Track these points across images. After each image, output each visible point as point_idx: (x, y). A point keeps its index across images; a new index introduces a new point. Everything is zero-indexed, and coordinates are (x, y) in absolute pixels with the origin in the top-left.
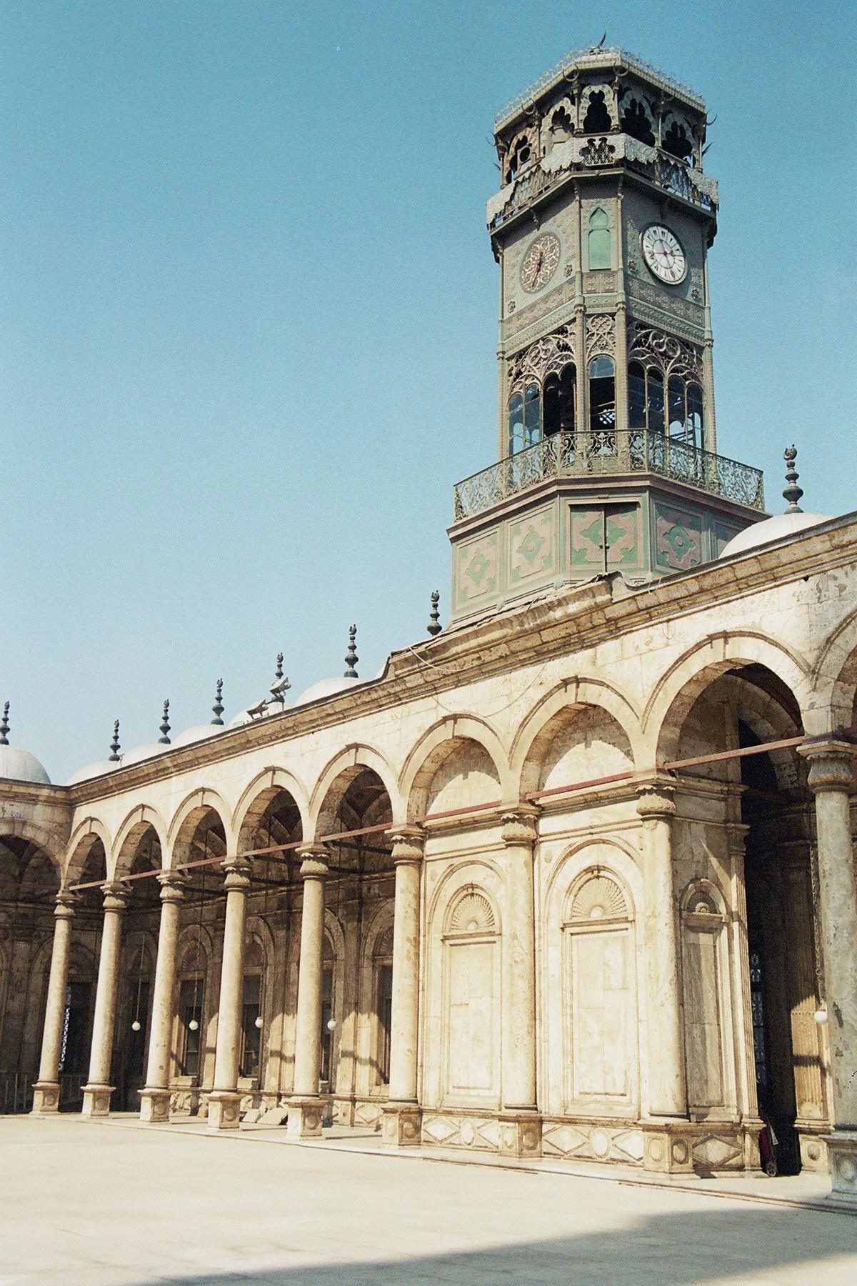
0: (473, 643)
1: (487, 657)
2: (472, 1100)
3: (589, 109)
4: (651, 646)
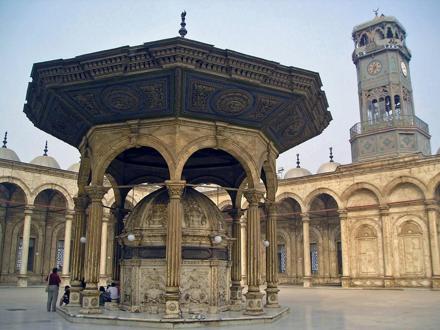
0: (371, 165)
1: (374, 169)
2: (369, 275)
3: (388, 31)
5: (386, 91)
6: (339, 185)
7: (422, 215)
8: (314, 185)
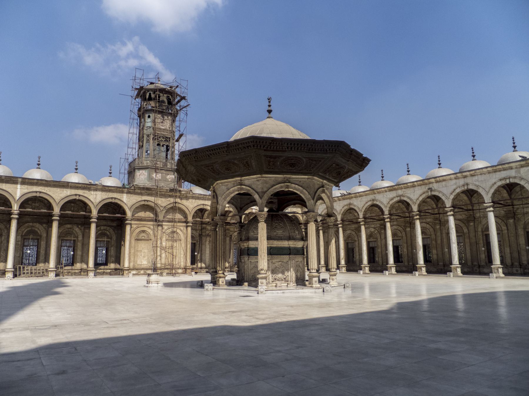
7: (182, 228)
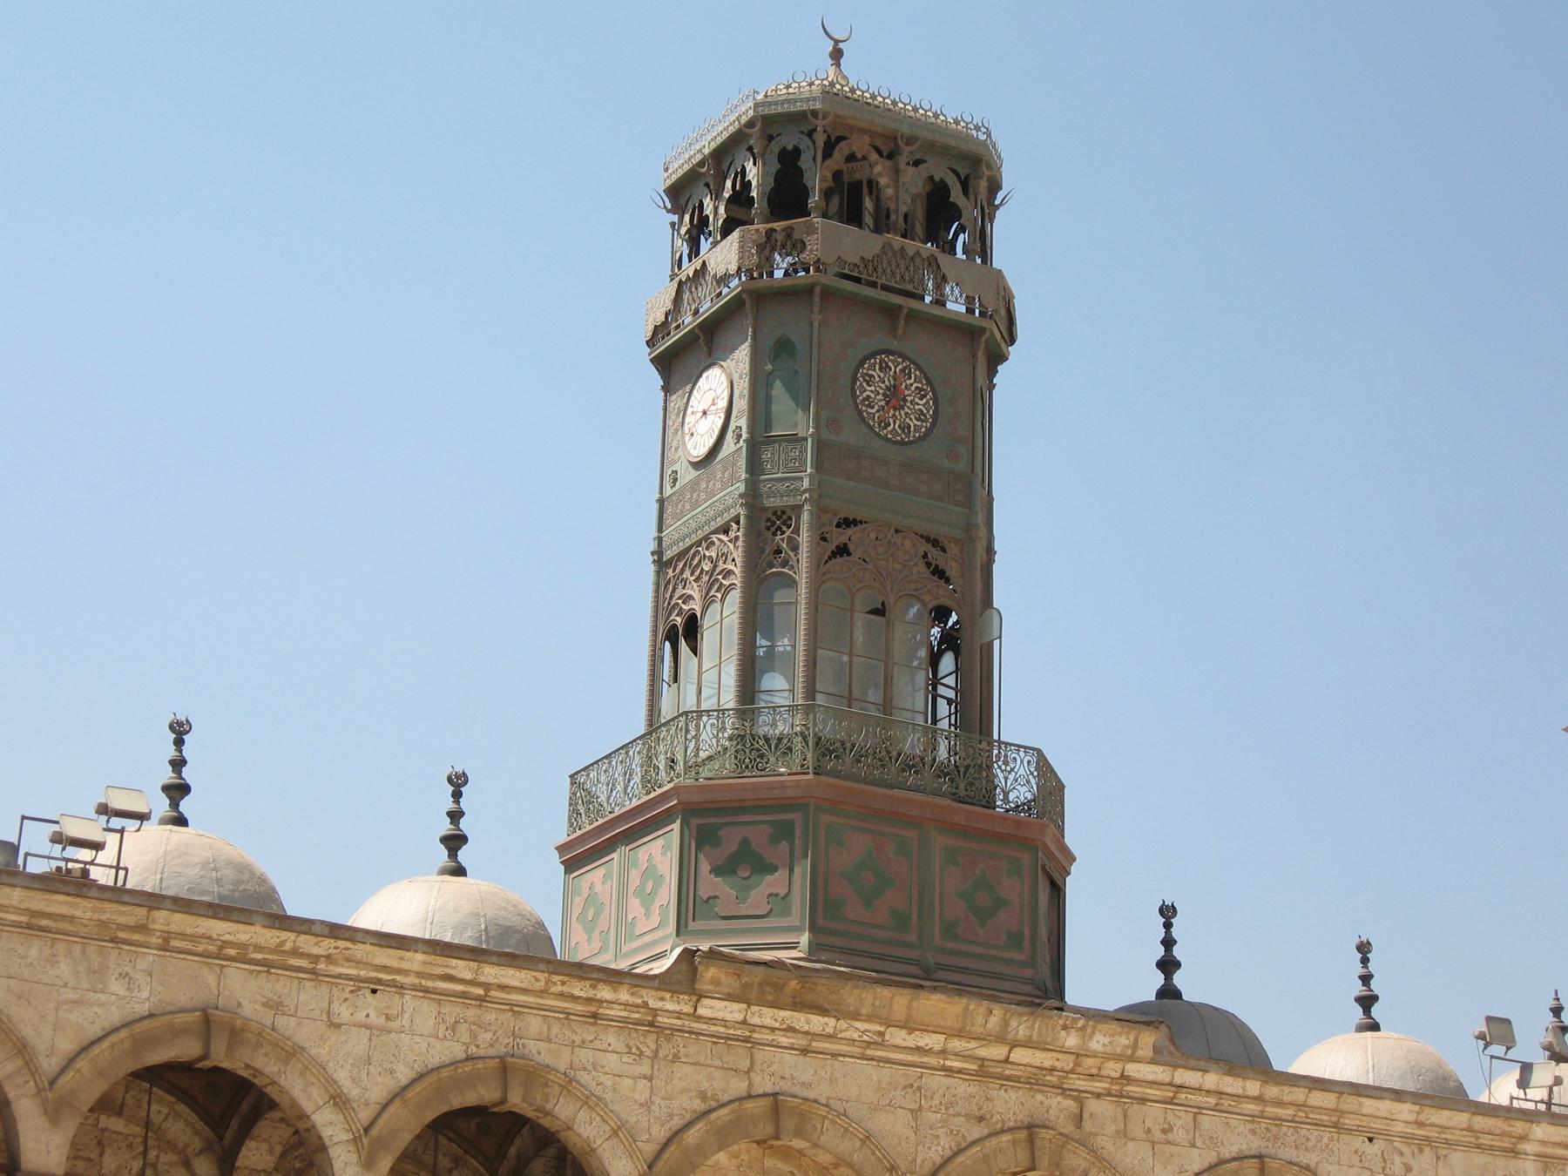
4: (1170, 1137)
5: (939, 573)
6: (650, 1079)
8: (463, 1028)
